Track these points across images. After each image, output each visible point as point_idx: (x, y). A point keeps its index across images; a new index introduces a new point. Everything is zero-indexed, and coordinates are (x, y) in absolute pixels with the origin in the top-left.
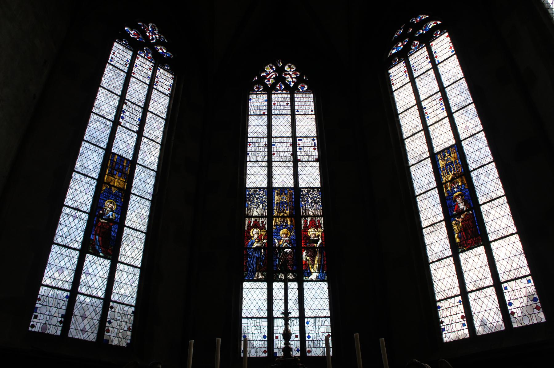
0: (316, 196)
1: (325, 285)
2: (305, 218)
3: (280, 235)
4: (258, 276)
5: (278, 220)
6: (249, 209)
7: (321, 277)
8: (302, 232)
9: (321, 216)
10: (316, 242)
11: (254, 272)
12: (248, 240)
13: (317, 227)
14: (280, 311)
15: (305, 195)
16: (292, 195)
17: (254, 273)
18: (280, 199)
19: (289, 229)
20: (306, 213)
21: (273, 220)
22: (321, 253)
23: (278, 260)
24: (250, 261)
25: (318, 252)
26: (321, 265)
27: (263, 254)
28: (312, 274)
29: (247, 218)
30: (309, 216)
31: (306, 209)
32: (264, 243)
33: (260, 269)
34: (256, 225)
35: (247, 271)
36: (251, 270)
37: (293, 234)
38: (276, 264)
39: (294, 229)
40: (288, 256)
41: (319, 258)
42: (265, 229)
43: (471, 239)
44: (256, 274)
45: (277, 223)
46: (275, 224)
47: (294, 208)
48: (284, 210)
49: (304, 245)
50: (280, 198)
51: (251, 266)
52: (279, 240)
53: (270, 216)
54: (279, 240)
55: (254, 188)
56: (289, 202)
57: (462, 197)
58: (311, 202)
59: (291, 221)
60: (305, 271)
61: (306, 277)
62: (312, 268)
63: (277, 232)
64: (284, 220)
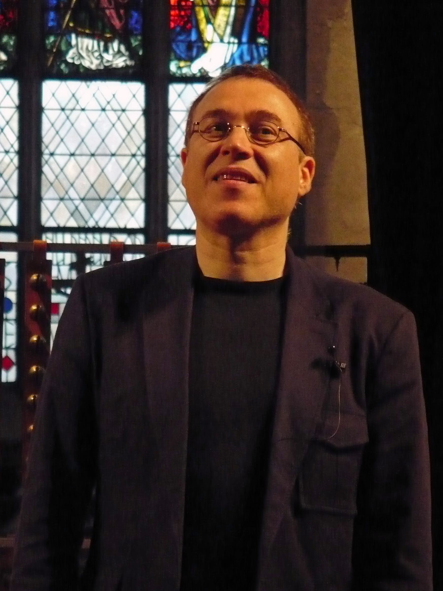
14: (69, 203)
26: (245, 14)
28: (204, 50)
60: (179, 34)
61: (179, 59)
62: (208, 21)
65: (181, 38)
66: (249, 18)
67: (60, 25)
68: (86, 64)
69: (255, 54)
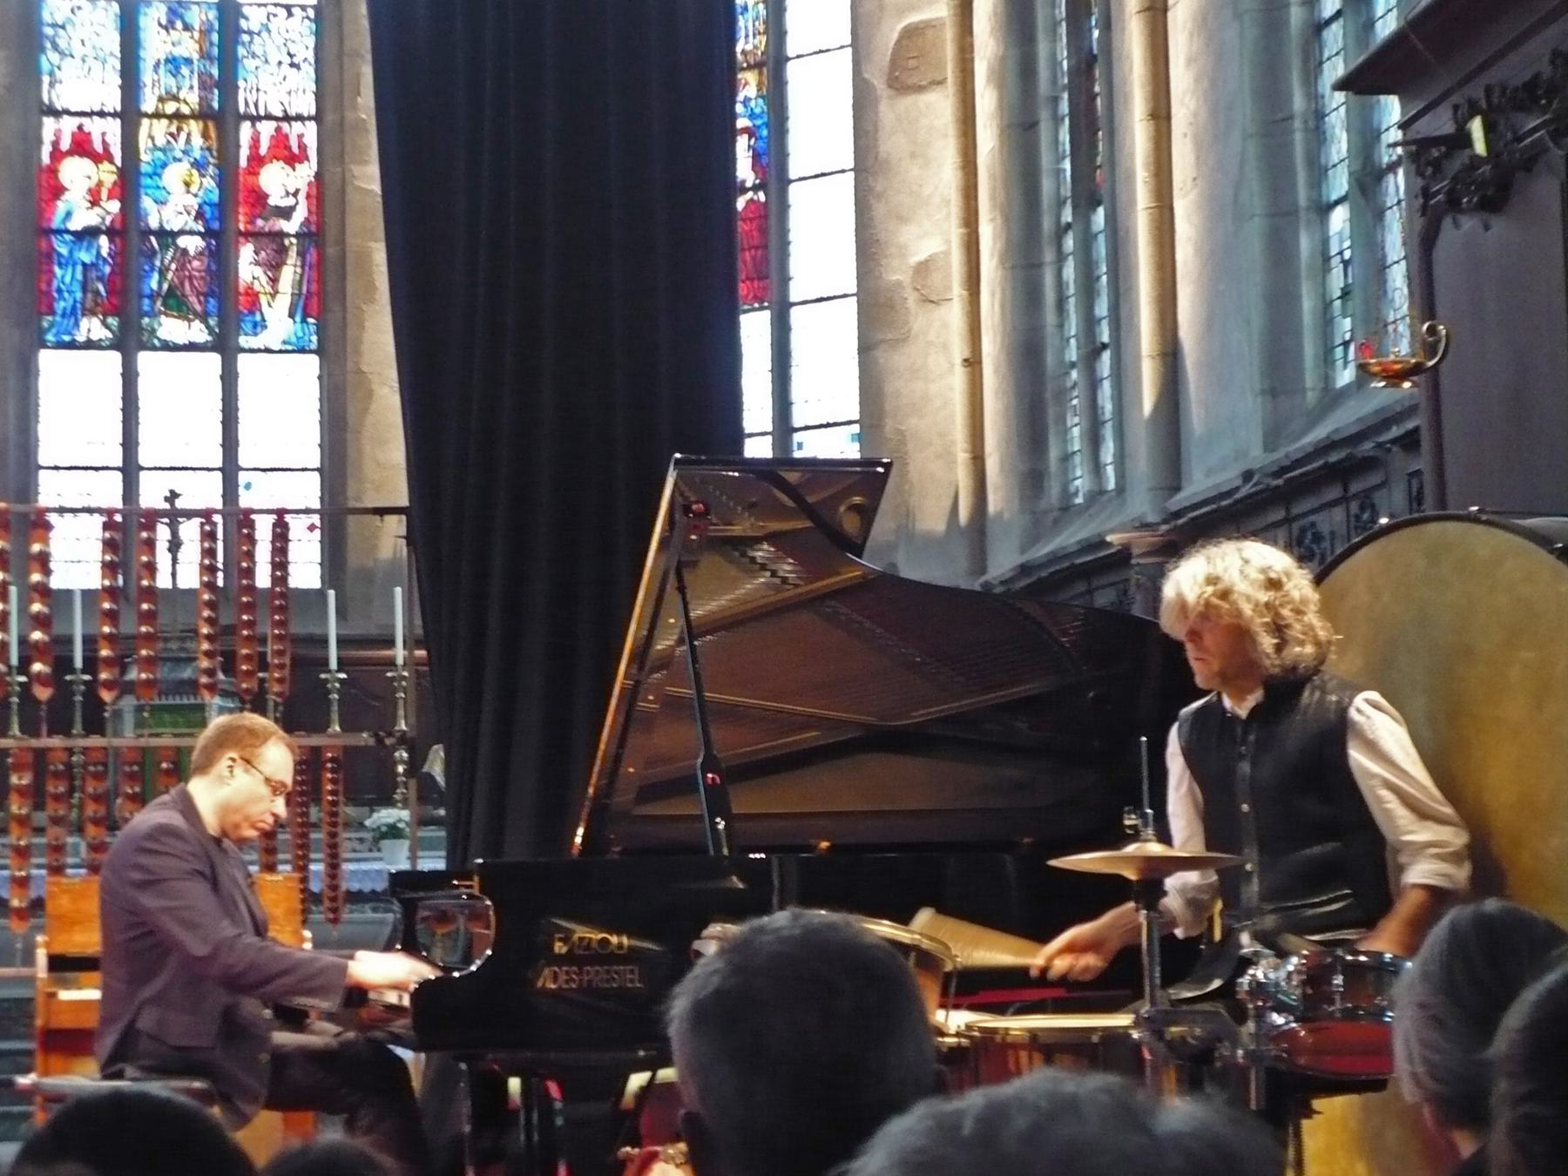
0: (296, 37)
2: (253, 125)
5: (160, 128)
7: (298, 338)
8: (241, 179)
9: (310, 118)
10: (286, 213)
11: (73, 314)
13: (293, 159)
19: (197, 165)
20: (256, 105)
22: (302, 254)
23: (156, 276)
24: (63, 277)
25: (293, 253)
26: (298, 300)
30: (269, 117)
31: (258, 90)
33: (97, 304)
34: (82, 145)
35: (52, 312)
36: (65, 308)
37: (209, 183)
38: (152, 290)
39: (214, 165)
41: (295, 272)
42: (111, 161)
43: (748, 282)
45: (152, 138)
46: (150, 145)
47: (218, 85)
48: (179, 88)
52: (161, 203)
53: (130, 115)
54: (161, 203)
57: (749, 139)
59: (205, 135)
61: (246, 334)
62: (270, 306)
63: (156, 174)
64: (179, 129)
65: (248, 318)
66: (301, 304)
67: (153, 309)
69: (306, 331)
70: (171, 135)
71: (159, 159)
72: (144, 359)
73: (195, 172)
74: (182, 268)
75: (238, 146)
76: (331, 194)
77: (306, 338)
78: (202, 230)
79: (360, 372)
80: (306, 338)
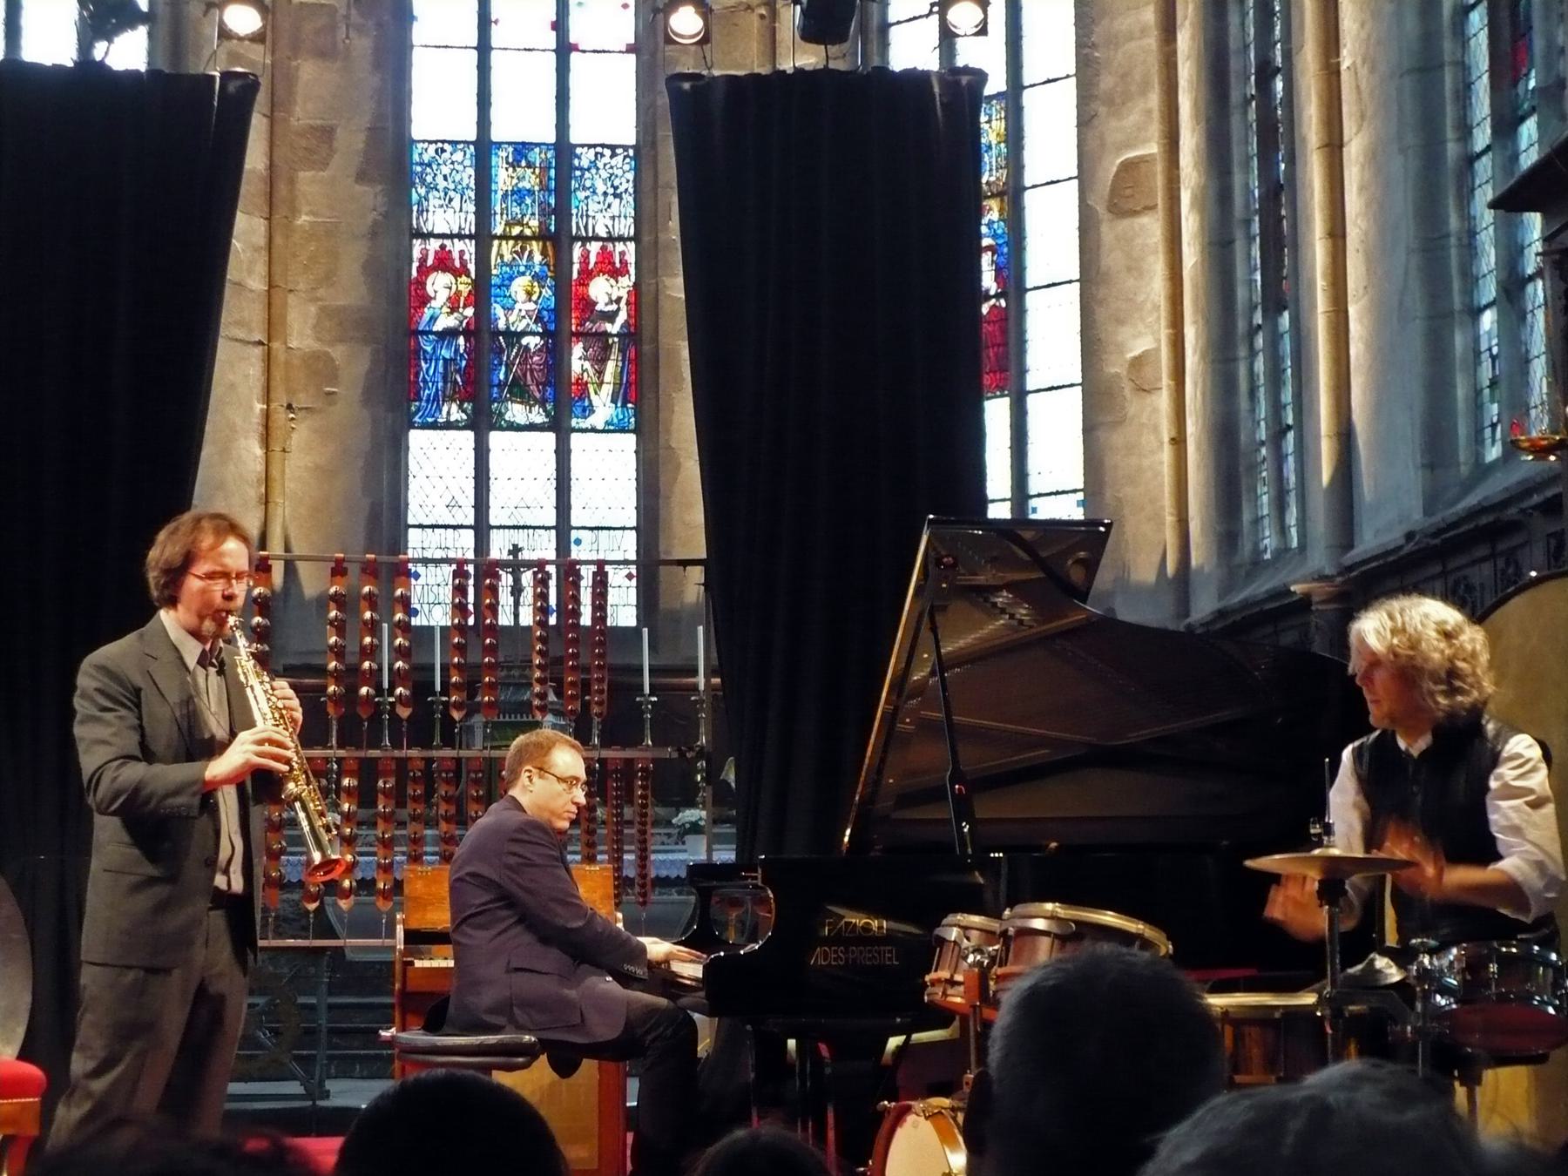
0: (619, 172)
1: (628, 443)
2: (583, 245)
3: (510, 296)
4: (449, 413)
5: (507, 248)
6: (423, 211)
7: (619, 420)
8: (573, 288)
9: (629, 239)
10: (611, 317)
12: (419, 308)
13: (616, 273)
15: (588, 169)
16: (549, 168)
17: (438, 404)
18: (515, 181)
19: (536, 277)
21: (491, 246)
22: (622, 350)
23: (503, 368)
24: (428, 370)
25: (615, 349)
27: (465, 350)
28: (594, 412)
29: (417, 238)
30: (596, 238)
31: (587, 216)
32: (466, 317)
33: (455, 392)
34: (443, 262)
35: (420, 400)
36: (429, 395)
37: (547, 292)
40: (532, 358)
42: (468, 275)
43: (992, 375)
44: (445, 409)
46: (499, 261)
47: (554, 211)
48: (523, 215)
49: (577, 325)
50: (512, 177)
51: (430, 384)
52: (508, 309)
53: (482, 237)
54: (508, 309)
55: (436, 142)
56: (539, 192)
57: (993, 256)
58: (605, 194)
59: (544, 253)
62: (596, 393)
63: (504, 286)
64: (523, 249)
66: (622, 391)
68: (518, 421)
70: (516, 252)
71: (506, 273)
72: (496, 439)
73: (536, 284)
74: (524, 362)
75: (572, 263)
76: (646, 299)
77: (626, 420)
78: (541, 330)
79: (670, 447)
80: (626, 420)
